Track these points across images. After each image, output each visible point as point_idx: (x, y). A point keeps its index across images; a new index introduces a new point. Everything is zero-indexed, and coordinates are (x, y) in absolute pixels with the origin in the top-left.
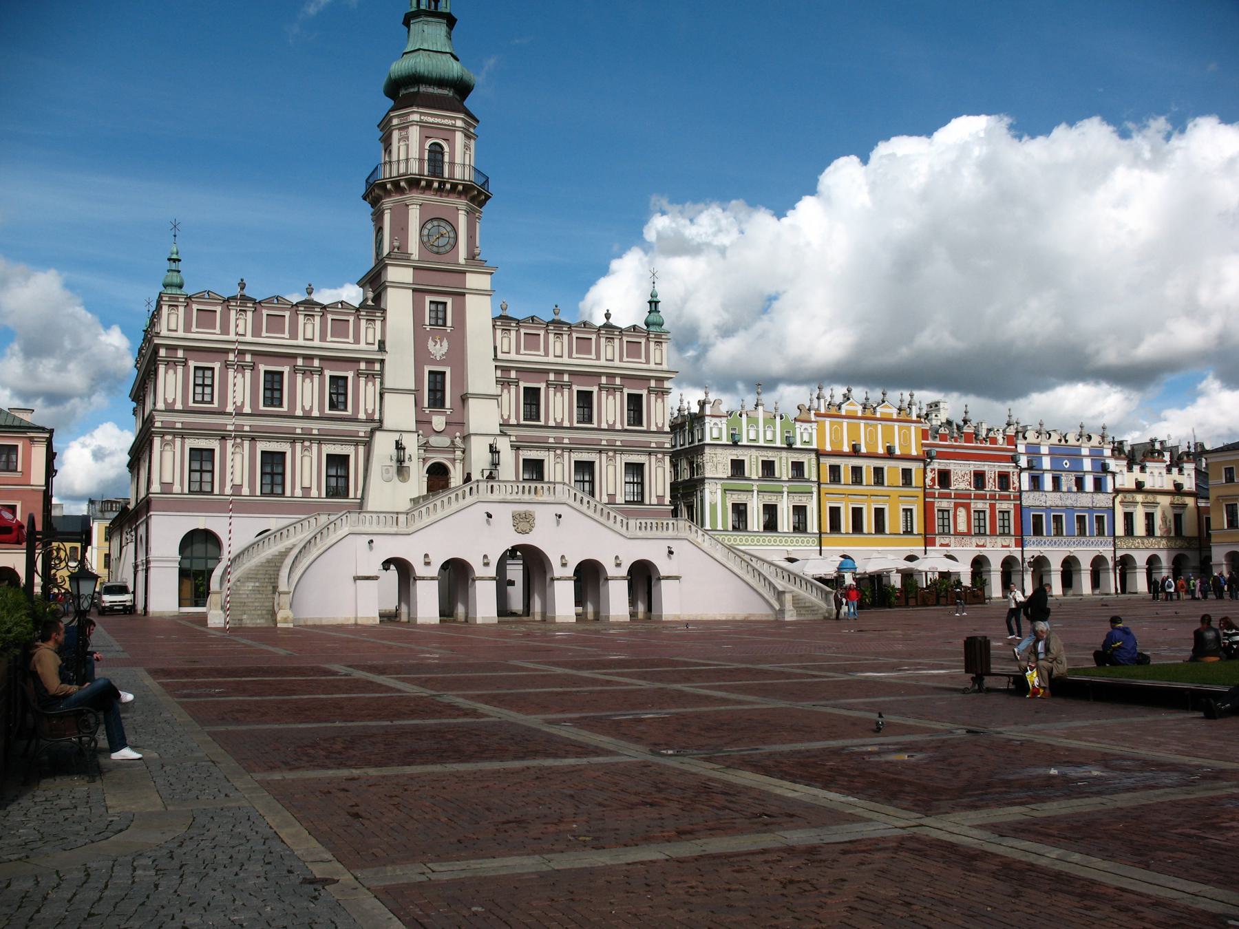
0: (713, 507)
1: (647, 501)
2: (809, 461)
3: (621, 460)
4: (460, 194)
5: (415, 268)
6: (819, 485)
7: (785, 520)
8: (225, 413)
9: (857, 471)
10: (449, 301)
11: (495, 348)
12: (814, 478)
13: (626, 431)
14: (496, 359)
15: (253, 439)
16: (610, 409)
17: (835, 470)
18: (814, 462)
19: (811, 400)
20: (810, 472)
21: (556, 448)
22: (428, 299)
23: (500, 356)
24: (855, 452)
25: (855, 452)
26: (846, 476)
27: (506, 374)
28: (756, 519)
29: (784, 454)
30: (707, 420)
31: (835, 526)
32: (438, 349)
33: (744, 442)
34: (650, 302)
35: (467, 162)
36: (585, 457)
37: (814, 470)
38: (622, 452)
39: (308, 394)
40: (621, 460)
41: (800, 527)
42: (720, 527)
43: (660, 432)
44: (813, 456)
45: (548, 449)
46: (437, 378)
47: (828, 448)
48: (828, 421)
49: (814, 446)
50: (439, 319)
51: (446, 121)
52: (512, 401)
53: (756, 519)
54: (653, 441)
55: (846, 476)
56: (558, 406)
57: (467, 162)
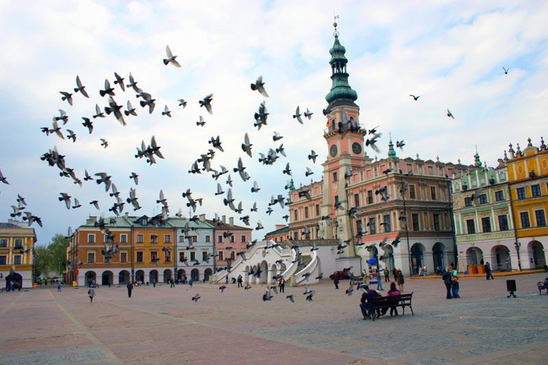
0: (458, 223)
2: (505, 190)
6: (511, 203)
7: (495, 224)
9: (536, 188)
12: (508, 199)
17: (521, 191)
18: (507, 189)
19: (505, 155)
20: (506, 196)
24: (533, 176)
25: (533, 176)
26: (529, 193)
28: (478, 226)
29: (490, 190)
30: (452, 181)
31: (526, 224)
32: (335, 187)
33: (470, 188)
34: (390, 146)
37: (508, 194)
41: (503, 225)
42: (462, 233)
44: (507, 186)
47: (516, 178)
48: (514, 165)
49: (507, 180)
53: (478, 226)
55: (529, 193)
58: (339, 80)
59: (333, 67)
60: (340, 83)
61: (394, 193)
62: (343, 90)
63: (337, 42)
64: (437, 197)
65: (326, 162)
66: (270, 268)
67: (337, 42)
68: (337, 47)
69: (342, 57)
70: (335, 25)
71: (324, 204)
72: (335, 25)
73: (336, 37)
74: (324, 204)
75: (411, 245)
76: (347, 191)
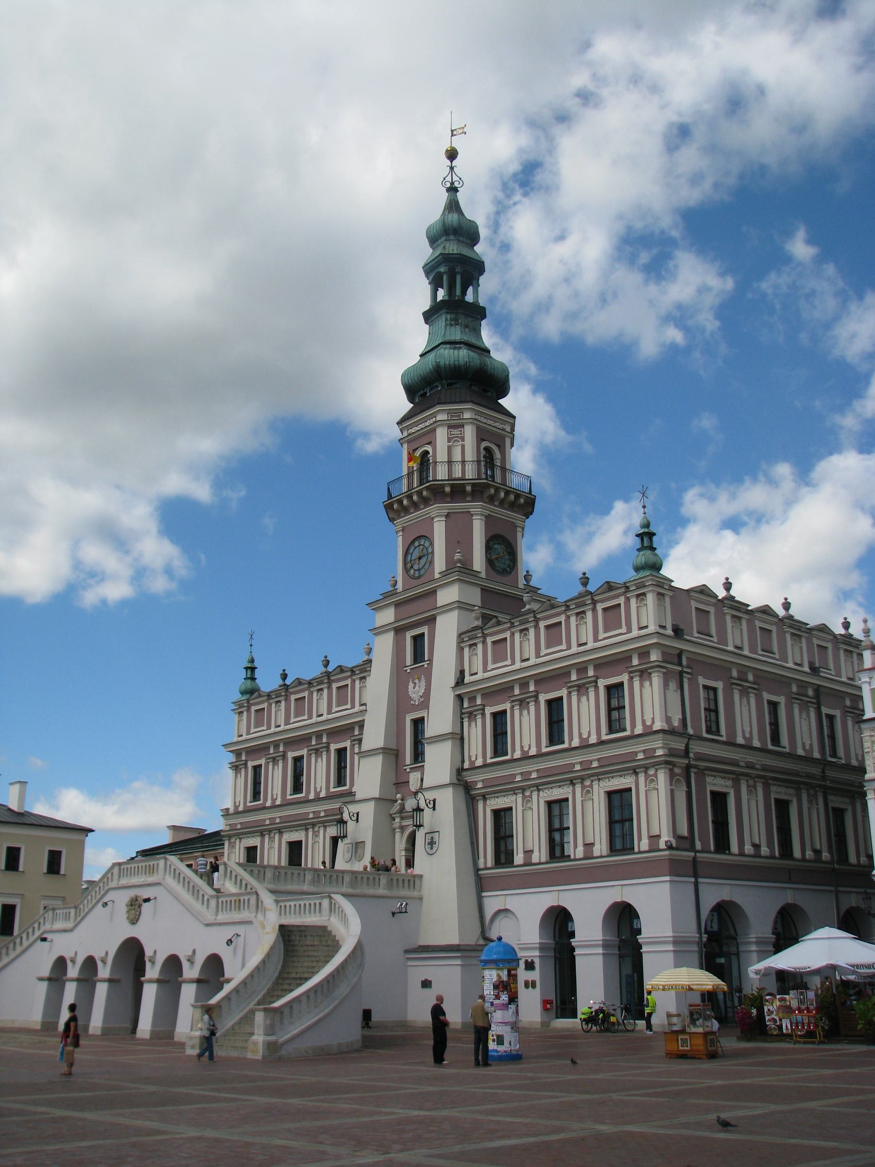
1: (636, 850)
3: (599, 790)
4: (426, 502)
5: (398, 605)
8: (265, 808)
10: (425, 629)
11: (462, 672)
13: (602, 743)
14: (460, 682)
15: (281, 833)
16: (585, 716)
21: (523, 789)
22: (409, 635)
23: (467, 679)
27: (466, 704)
35: (457, 457)
36: (557, 793)
38: (599, 776)
39: (320, 774)
40: (599, 790)
43: (649, 732)
45: (514, 791)
46: (418, 724)
50: (418, 656)
51: (427, 424)
52: (478, 735)
54: (638, 749)
56: (527, 729)
57: (457, 457)
58: (455, 322)
59: (436, 284)
60: (456, 334)
61: (651, 703)
62: (463, 355)
63: (453, 206)
64: (784, 740)
65: (386, 595)
66: (152, 972)
67: (453, 206)
68: (453, 218)
69: (466, 252)
70: (452, 155)
71: (365, 747)
72: (452, 155)
73: (453, 190)
74: (365, 747)
75: (707, 906)
76: (460, 698)
